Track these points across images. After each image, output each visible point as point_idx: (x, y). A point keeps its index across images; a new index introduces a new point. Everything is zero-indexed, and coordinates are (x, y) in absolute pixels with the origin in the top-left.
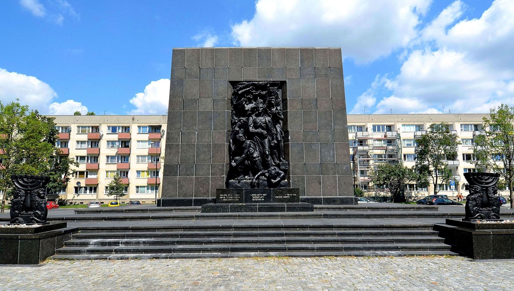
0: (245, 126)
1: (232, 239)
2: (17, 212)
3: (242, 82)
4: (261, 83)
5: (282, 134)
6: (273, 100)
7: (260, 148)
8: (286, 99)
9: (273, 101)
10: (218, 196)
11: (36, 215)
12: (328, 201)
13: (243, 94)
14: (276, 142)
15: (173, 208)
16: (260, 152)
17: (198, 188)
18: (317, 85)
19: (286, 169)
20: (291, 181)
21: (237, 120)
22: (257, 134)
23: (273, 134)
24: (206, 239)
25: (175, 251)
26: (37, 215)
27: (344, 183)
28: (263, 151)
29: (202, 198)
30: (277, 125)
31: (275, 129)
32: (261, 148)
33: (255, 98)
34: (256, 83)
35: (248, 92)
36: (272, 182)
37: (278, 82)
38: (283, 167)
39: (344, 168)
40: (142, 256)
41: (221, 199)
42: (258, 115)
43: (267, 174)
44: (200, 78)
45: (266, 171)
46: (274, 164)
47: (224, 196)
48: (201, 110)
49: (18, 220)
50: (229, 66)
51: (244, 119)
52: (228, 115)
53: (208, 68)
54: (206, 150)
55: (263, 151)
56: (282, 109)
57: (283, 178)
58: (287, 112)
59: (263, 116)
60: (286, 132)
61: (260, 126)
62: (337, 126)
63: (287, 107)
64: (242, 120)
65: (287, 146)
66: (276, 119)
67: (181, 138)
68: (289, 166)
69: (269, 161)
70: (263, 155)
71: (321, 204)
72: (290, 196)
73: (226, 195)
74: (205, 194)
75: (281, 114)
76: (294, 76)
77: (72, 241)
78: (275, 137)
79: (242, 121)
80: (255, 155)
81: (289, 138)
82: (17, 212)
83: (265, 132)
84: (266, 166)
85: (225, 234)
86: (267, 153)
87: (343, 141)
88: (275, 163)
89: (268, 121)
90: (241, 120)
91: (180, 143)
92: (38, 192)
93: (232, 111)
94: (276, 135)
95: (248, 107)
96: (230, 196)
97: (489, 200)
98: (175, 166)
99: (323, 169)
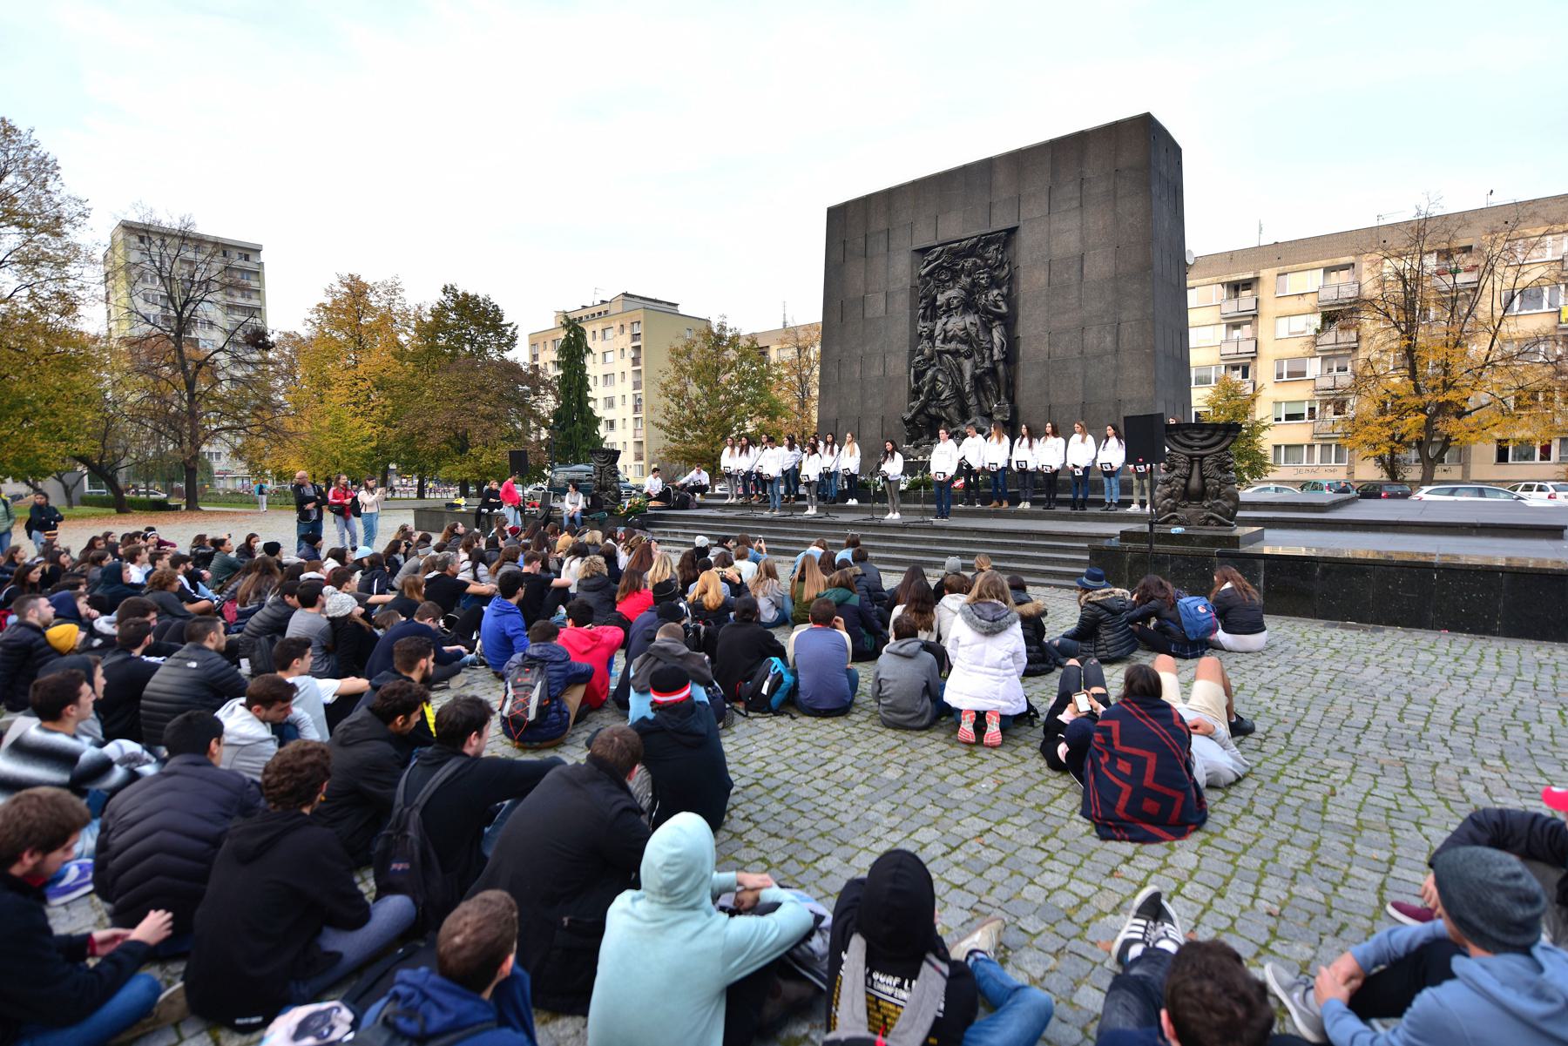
13: (930, 274)
22: (948, 352)
33: (955, 277)
66: (989, 318)
70: (959, 393)
80: (943, 397)
83: (963, 348)
94: (991, 350)
97: (1204, 486)
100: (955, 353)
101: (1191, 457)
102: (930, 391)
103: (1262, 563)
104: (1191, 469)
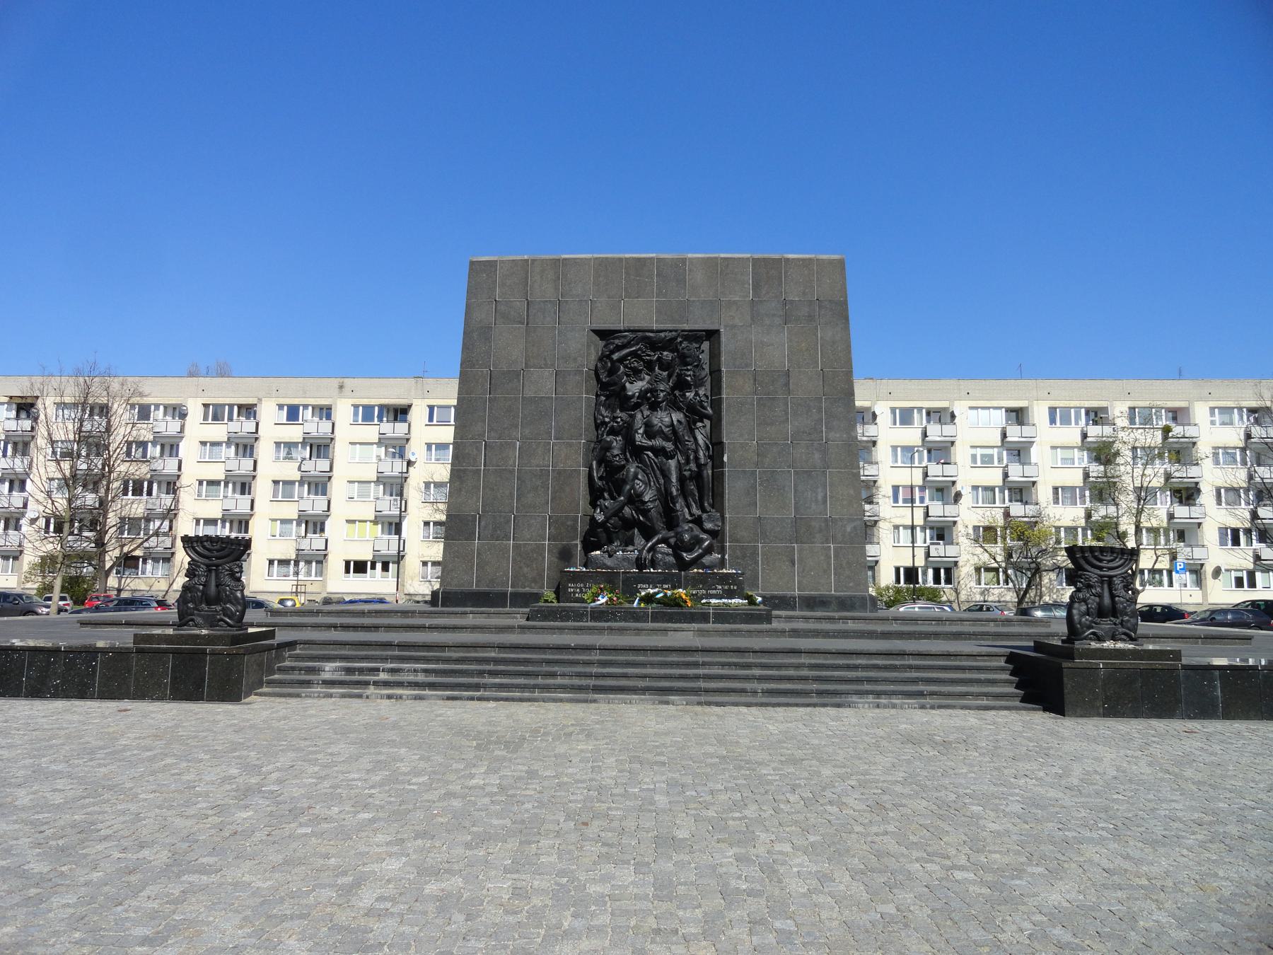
0: (627, 431)
1: (595, 670)
2: (191, 605)
3: (620, 331)
4: (662, 335)
5: (708, 448)
6: (689, 373)
7: (658, 482)
8: (720, 371)
9: (690, 375)
11: (226, 612)
12: (811, 603)
13: (621, 360)
14: (693, 466)
15: (468, 609)
16: (659, 490)
17: (521, 568)
18: (790, 340)
19: (716, 528)
20: (727, 557)
21: (607, 417)
22: (652, 449)
23: (689, 449)
24: (546, 668)
25: (485, 687)
26: (229, 613)
27: (848, 563)
28: (666, 489)
29: (527, 589)
31: (692, 439)
32: (662, 481)
34: (651, 335)
35: (634, 354)
36: (683, 558)
38: (709, 526)
40: (424, 695)
41: (571, 593)
42: (654, 407)
43: (672, 541)
44: (527, 324)
45: (672, 534)
46: (690, 518)
47: (577, 588)
48: (529, 393)
49: (192, 620)
51: (624, 415)
52: (588, 406)
53: (547, 301)
54: (539, 483)
55: (666, 489)
56: (709, 394)
57: (709, 550)
58: (720, 401)
59: (665, 410)
60: (716, 446)
61: (660, 433)
62: (833, 433)
63: (720, 388)
64: (620, 417)
65: (718, 478)
67: (485, 456)
68: (723, 523)
69: (677, 511)
70: (665, 498)
71: (793, 608)
74: (534, 581)
75: (706, 404)
77: (287, 663)
78: (692, 457)
79: (619, 420)
81: (725, 459)
82: (191, 605)
83: (669, 446)
84: (671, 520)
85: (582, 660)
87: (846, 467)
88: (691, 515)
89: (678, 421)
90: (618, 417)
91: (482, 468)
92: (231, 570)
93: (597, 396)
94: (696, 452)
95: (634, 388)
98: (470, 518)
99: (801, 530)
100: (658, 451)
101: (1102, 576)
102: (630, 490)
103: (1217, 673)
104: (1102, 589)
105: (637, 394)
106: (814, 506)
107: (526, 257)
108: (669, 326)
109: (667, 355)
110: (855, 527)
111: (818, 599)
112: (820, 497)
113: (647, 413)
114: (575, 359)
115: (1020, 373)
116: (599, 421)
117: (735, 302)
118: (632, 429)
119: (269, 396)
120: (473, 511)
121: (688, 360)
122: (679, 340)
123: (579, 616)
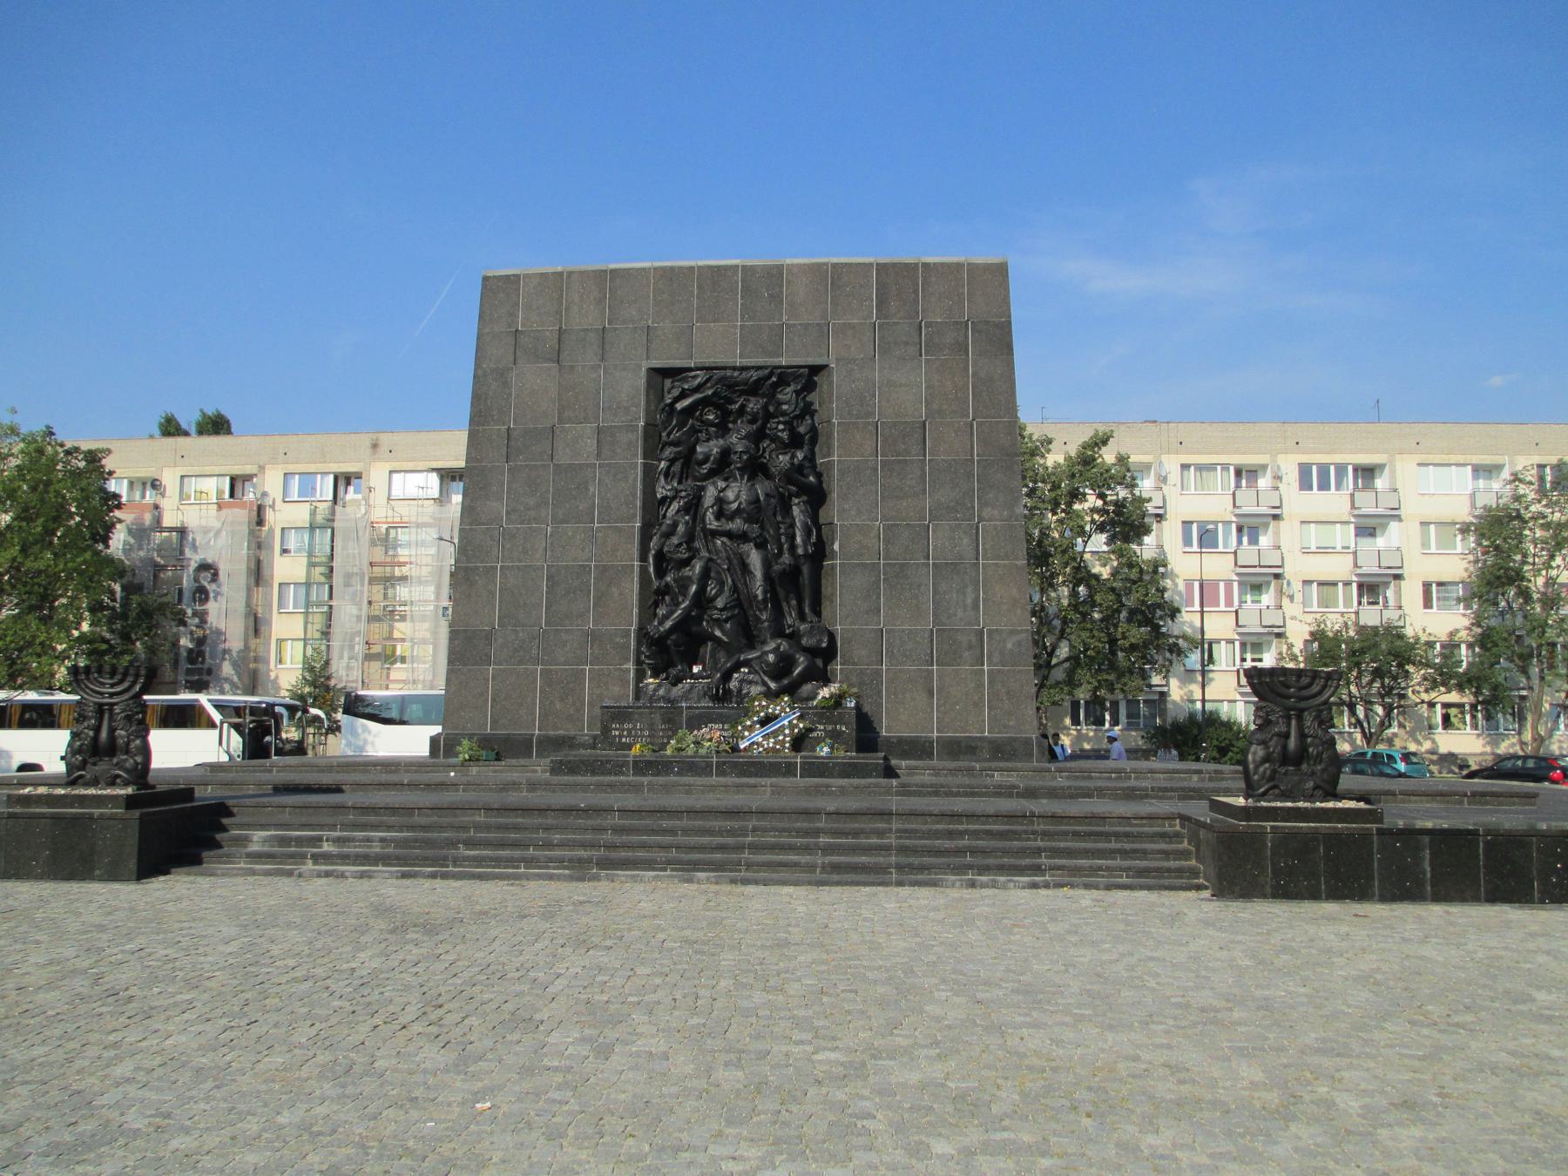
0: (693, 506)
3: (690, 370)
4: (745, 375)
8: (829, 421)
9: (783, 430)
10: (606, 730)
12: (957, 749)
14: (786, 558)
22: (729, 534)
30: (796, 505)
35: (705, 402)
37: (802, 370)
39: (1009, 646)
41: (615, 736)
50: (650, 322)
62: (990, 509)
72: (825, 730)
73: (631, 726)
76: (852, 349)
79: (683, 494)
81: (836, 547)
86: (760, 598)
87: (1006, 557)
89: (767, 495)
94: (793, 537)
95: (710, 448)
96: (641, 730)
103: (1426, 839)
104: (1289, 725)
105: (712, 458)
106: (960, 613)
107: (560, 269)
108: (760, 361)
109: (754, 405)
110: (1019, 643)
111: (963, 745)
112: (969, 601)
113: (721, 484)
114: (627, 409)
115: (1377, 413)
116: (659, 496)
117: (852, 327)
118: (702, 506)
119: (274, 461)
120: (486, 626)
121: (785, 407)
122: (774, 379)
123: (619, 768)
